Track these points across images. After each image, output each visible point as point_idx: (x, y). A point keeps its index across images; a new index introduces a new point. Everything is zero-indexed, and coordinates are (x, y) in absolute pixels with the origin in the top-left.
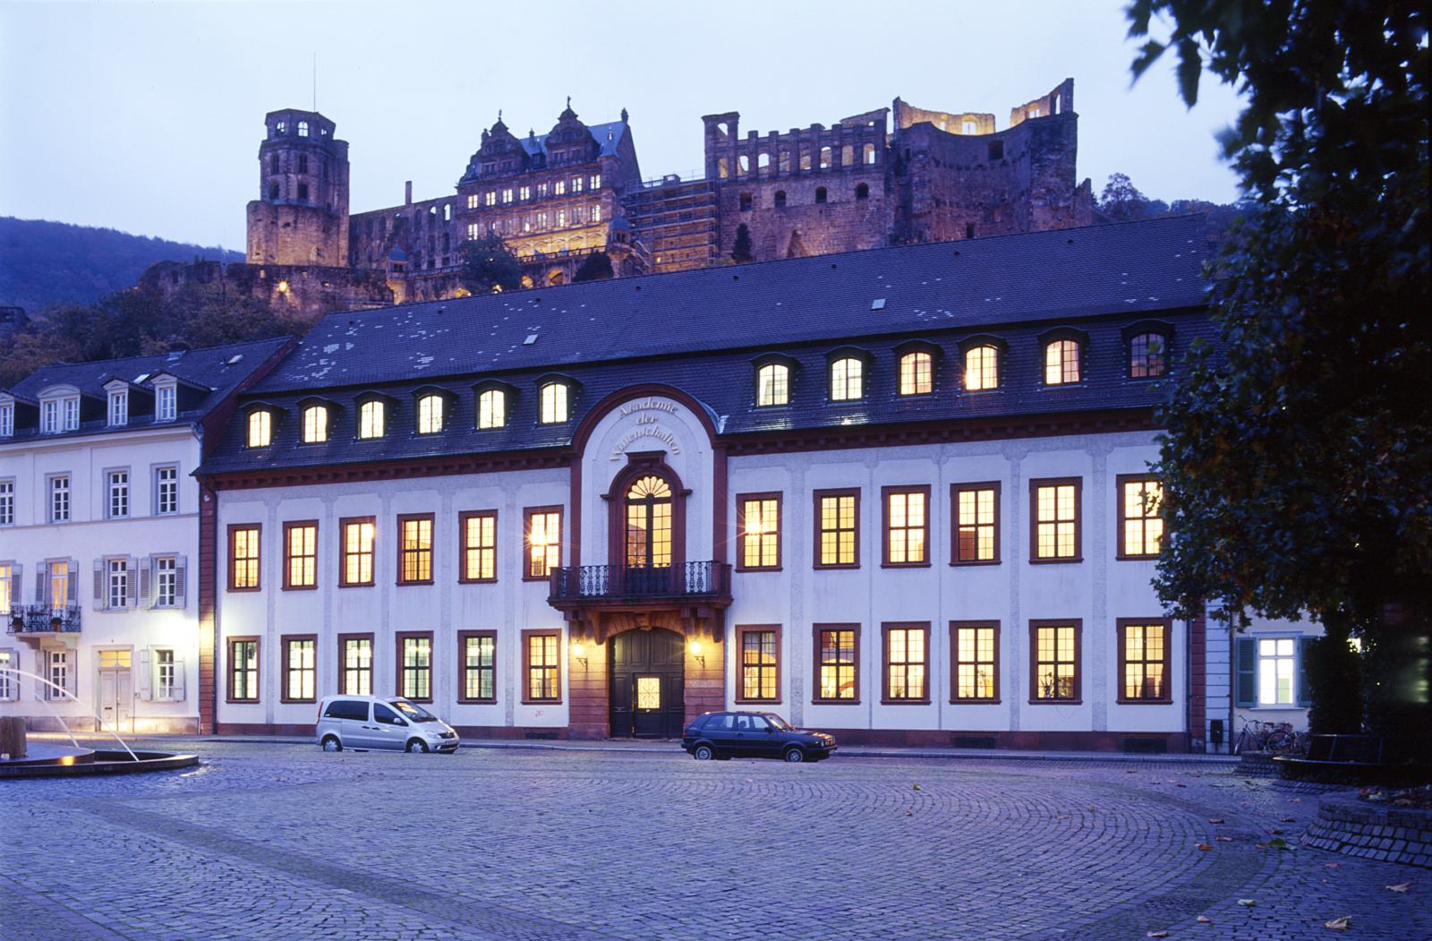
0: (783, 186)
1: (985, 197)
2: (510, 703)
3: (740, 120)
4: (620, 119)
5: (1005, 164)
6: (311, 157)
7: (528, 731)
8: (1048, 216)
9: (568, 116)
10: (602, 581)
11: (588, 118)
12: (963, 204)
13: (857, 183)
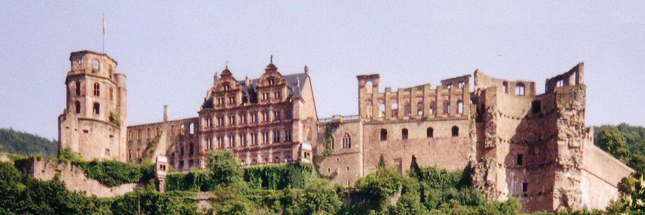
0: (407, 126)
4: (303, 71)
5: (541, 116)
9: (272, 68)
11: (284, 69)
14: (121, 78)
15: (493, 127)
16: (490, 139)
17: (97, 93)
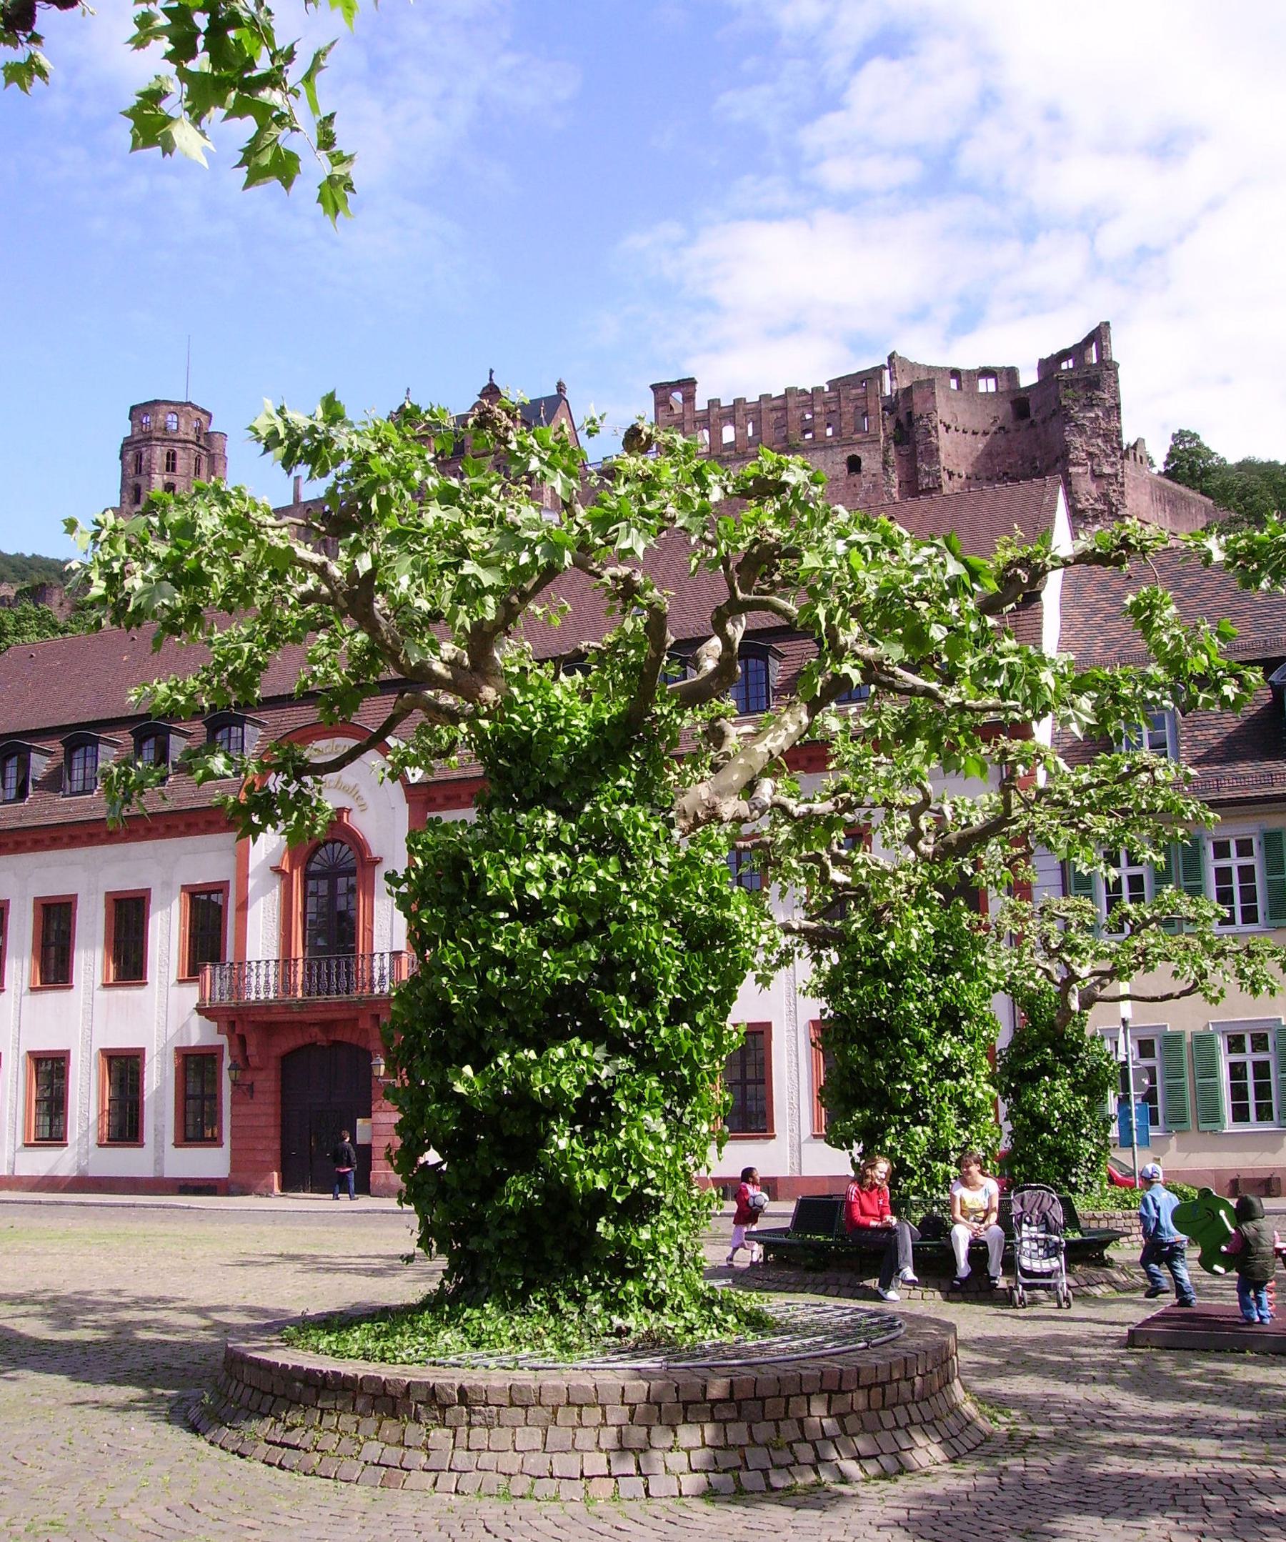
1: (1011, 466)
2: (159, 1146)
3: (698, 387)
4: (555, 393)
5: (1032, 424)
6: (180, 453)
7: (182, 1183)
8: (1093, 487)
10: (272, 980)
12: (983, 475)
13: (846, 455)
14: (217, 442)
15: (933, 452)
16: (928, 474)
17: (171, 467)
